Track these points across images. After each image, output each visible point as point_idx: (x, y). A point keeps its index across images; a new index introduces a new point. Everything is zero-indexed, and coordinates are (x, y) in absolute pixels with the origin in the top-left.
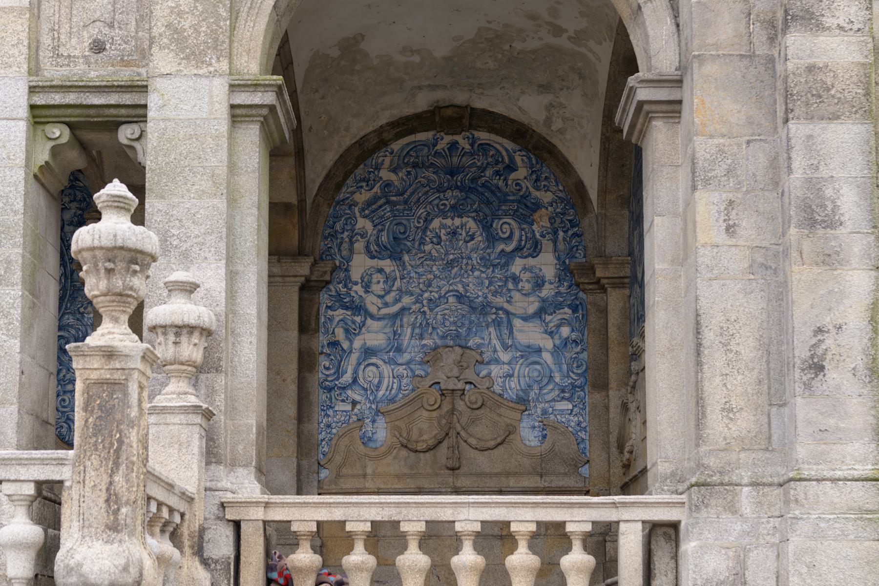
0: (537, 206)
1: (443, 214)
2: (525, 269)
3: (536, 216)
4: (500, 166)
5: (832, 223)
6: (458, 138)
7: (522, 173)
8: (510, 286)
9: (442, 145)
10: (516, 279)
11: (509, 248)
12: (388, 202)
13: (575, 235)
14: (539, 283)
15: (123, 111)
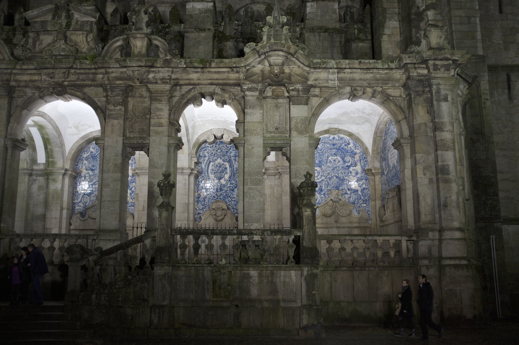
0: (356, 154)
1: (332, 155)
2: (353, 170)
3: (356, 156)
4: (346, 143)
5: (448, 173)
6: (335, 136)
7: (351, 145)
8: (350, 174)
9: (331, 138)
10: (351, 172)
11: (349, 164)
12: (318, 152)
13: (366, 161)
14: (357, 174)
15: (284, 145)
